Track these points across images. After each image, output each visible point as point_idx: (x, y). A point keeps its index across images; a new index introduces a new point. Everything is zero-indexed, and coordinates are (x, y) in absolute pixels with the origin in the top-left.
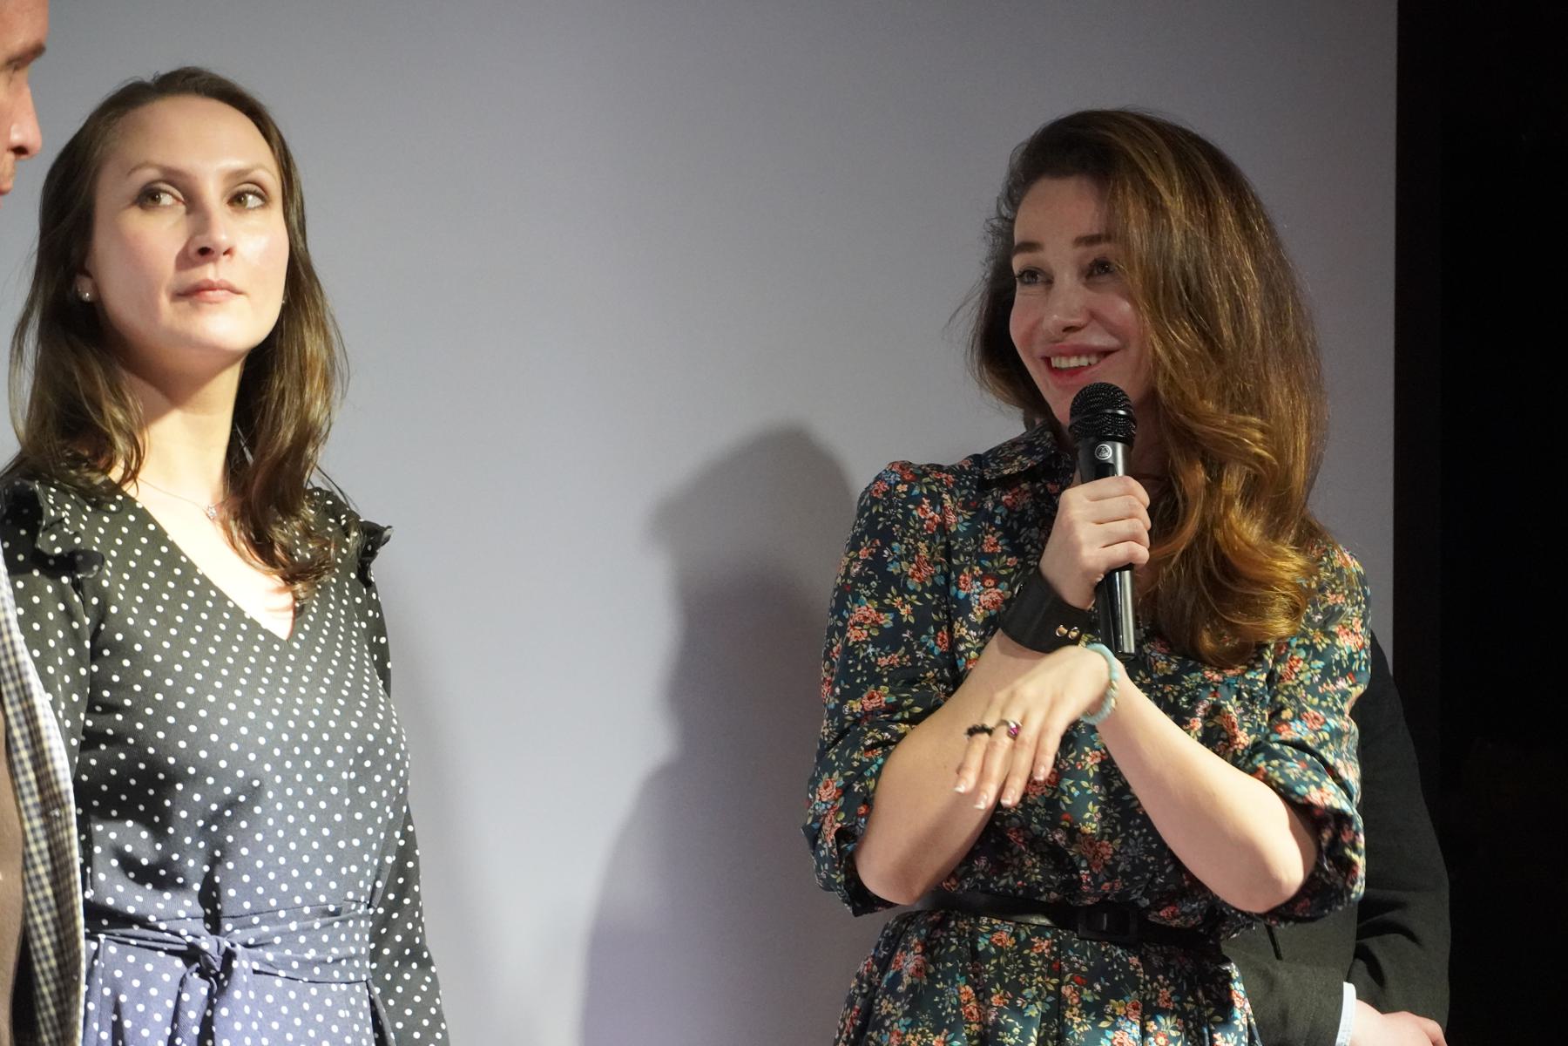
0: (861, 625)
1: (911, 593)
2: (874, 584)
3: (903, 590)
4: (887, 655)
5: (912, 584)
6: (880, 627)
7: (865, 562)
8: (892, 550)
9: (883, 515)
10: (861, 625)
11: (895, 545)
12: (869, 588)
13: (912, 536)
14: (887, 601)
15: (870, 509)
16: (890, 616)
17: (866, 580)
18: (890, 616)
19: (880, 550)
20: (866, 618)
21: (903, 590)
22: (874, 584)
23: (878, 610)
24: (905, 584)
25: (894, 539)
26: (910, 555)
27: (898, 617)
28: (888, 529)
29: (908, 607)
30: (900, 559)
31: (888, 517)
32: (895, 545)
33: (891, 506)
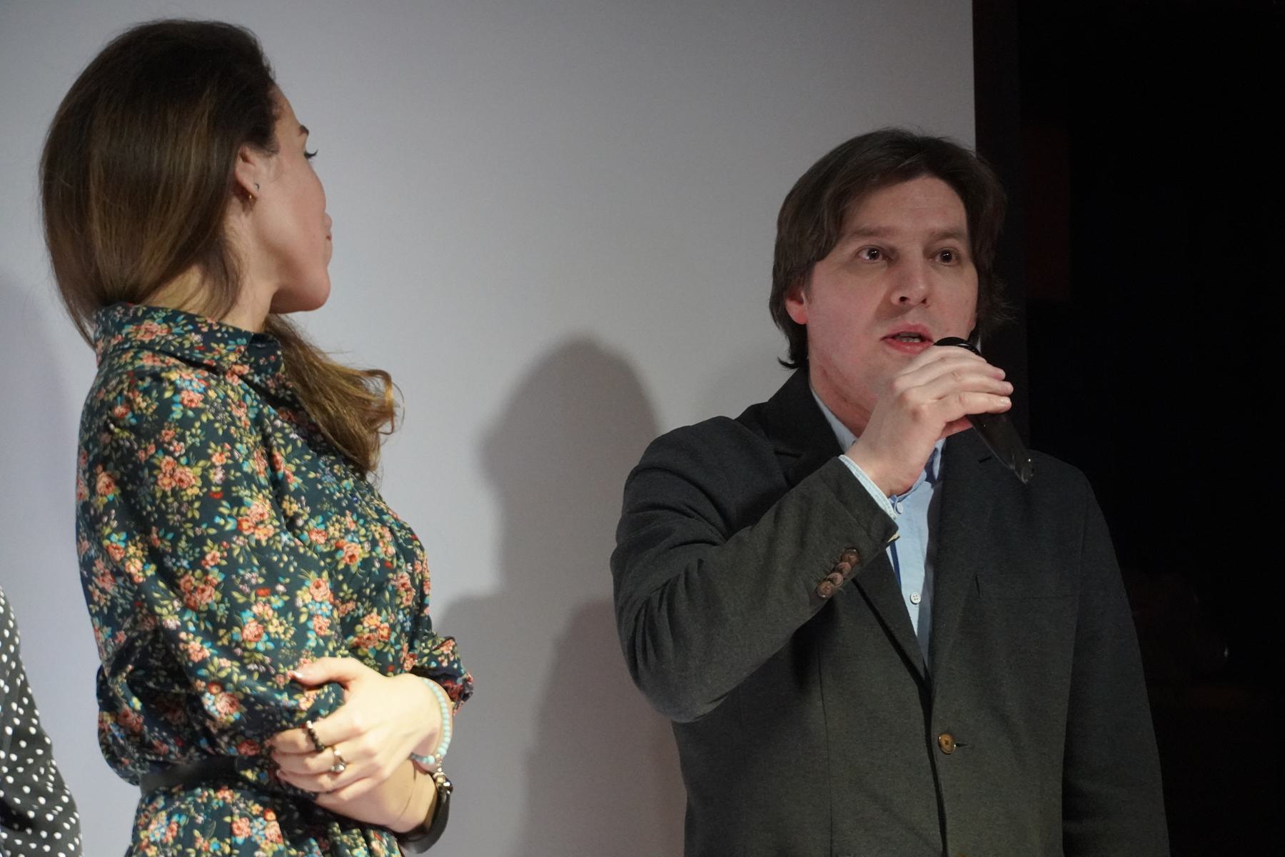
0: (262, 522)
1: (265, 488)
7: (226, 468)
20: (262, 515)
28: (226, 432)
30: (247, 458)
31: (222, 422)
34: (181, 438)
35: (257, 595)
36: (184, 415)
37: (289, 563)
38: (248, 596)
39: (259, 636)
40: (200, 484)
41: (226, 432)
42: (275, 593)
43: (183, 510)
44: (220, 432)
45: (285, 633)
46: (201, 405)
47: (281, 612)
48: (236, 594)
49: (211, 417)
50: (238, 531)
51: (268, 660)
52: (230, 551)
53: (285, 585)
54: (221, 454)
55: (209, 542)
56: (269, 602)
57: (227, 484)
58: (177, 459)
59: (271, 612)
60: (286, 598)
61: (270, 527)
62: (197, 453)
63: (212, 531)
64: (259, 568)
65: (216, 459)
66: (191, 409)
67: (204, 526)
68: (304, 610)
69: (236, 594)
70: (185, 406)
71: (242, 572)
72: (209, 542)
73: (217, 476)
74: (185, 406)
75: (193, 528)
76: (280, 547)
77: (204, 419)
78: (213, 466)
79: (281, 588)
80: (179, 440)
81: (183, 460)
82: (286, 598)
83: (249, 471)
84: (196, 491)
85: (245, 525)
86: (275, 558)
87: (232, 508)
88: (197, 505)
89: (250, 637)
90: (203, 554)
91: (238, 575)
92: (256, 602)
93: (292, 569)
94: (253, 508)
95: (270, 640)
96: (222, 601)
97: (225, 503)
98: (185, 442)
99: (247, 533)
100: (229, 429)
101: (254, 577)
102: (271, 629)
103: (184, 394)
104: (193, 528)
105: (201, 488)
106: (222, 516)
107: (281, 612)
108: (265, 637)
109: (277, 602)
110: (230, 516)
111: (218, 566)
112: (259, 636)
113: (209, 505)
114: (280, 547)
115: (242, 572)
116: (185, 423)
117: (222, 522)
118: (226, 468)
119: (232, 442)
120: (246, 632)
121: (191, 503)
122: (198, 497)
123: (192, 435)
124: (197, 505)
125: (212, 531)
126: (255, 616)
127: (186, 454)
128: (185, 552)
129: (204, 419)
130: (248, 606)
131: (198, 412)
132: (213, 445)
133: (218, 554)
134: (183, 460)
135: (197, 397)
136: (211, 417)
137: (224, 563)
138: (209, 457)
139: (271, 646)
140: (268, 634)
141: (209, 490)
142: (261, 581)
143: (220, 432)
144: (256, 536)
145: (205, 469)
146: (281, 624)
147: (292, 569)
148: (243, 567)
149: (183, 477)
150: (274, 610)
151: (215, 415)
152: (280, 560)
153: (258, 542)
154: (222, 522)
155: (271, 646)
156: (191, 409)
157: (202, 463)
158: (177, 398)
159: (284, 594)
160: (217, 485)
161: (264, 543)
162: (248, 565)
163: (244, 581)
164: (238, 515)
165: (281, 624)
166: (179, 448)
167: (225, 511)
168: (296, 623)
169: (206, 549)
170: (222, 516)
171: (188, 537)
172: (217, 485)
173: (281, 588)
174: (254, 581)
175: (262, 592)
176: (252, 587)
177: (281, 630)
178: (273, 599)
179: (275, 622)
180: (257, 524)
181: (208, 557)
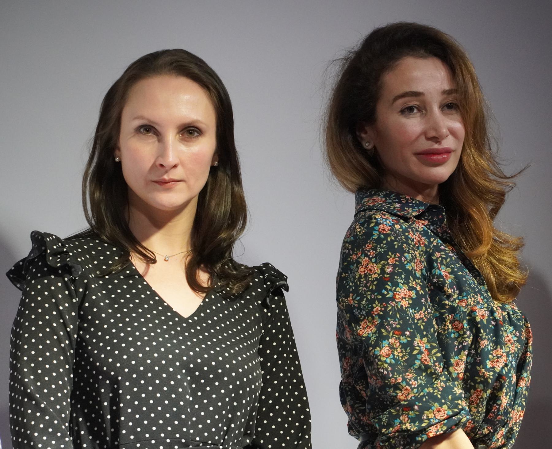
0: (405, 298)
1: (418, 279)
2: (403, 276)
3: (415, 278)
4: (418, 312)
5: (418, 274)
6: (412, 298)
7: (394, 266)
8: (405, 258)
9: (395, 241)
11: (406, 255)
12: (402, 279)
13: (413, 249)
14: (410, 284)
16: (414, 292)
17: (399, 274)
18: (414, 292)
19: (400, 258)
21: (415, 278)
22: (403, 276)
24: (415, 273)
25: (405, 252)
26: (414, 258)
27: (417, 292)
28: (400, 247)
29: (418, 286)
30: (410, 261)
32: (406, 255)
33: (398, 236)
34: (375, 249)
35: (394, 334)
36: (379, 236)
38: (389, 332)
39: (389, 355)
40: (379, 272)
41: (400, 247)
42: (404, 335)
43: (368, 285)
44: (396, 247)
45: (402, 357)
46: (389, 232)
47: (404, 346)
48: (383, 330)
49: (393, 239)
50: (393, 299)
51: (390, 369)
52: (386, 308)
54: (393, 259)
55: (376, 302)
56: (399, 339)
57: (393, 274)
58: (370, 259)
59: (398, 344)
60: (409, 339)
62: (381, 257)
63: (380, 297)
64: (399, 320)
65: (391, 261)
66: (383, 234)
67: (376, 294)
68: (417, 348)
69: (383, 330)
70: (380, 232)
71: (389, 319)
72: (376, 302)
73: (389, 269)
74: (380, 232)
75: (371, 295)
77: (389, 239)
78: (388, 264)
79: (407, 333)
80: (373, 250)
81: (373, 260)
82: (409, 339)
83: (410, 268)
84: (376, 276)
85: (397, 297)
87: (392, 287)
88: (375, 283)
89: (384, 354)
90: (373, 308)
91: (387, 320)
92: (392, 337)
94: (403, 289)
95: (394, 358)
96: (375, 333)
97: (389, 283)
98: (376, 250)
99: (397, 301)
100: (402, 245)
101: (395, 324)
102: (396, 353)
103: (381, 227)
104: (371, 295)
105: (379, 275)
106: (386, 289)
107: (404, 346)
108: (391, 356)
109: (404, 340)
110: (391, 290)
111: (378, 314)
112: (389, 355)
113: (381, 283)
115: (389, 319)
116: (379, 241)
117: (386, 293)
118: (394, 266)
119: (402, 252)
120: (383, 351)
121: (372, 282)
122: (376, 278)
123: (381, 248)
124: (375, 283)
125: (380, 297)
126: (389, 344)
127: (375, 257)
128: (364, 307)
129: (389, 239)
130: (387, 338)
131: (387, 235)
132: (390, 254)
133: (379, 309)
134: (373, 260)
135: (387, 228)
136: (393, 239)
137: (382, 313)
139: (393, 362)
140: (394, 355)
141: (383, 275)
142: (398, 326)
143: (396, 247)
144: (401, 303)
145: (384, 265)
146: (402, 352)
148: (391, 317)
149: (372, 268)
150: (400, 343)
151: (395, 237)
154: (386, 293)
155: (393, 362)
156: (383, 234)
157: (382, 262)
158: (377, 228)
159: (408, 337)
160: (388, 274)
162: (394, 317)
163: (389, 324)
164: (395, 290)
165: (402, 352)
166: (372, 253)
168: (410, 354)
169: (374, 305)
170: (386, 289)
171: (367, 299)
172: (388, 274)
173: (407, 333)
174: (394, 326)
175: (397, 332)
176: (392, 329)
177: (400, 355)
178: (402, 338)
179: (399, 350)
181: (375, 310)
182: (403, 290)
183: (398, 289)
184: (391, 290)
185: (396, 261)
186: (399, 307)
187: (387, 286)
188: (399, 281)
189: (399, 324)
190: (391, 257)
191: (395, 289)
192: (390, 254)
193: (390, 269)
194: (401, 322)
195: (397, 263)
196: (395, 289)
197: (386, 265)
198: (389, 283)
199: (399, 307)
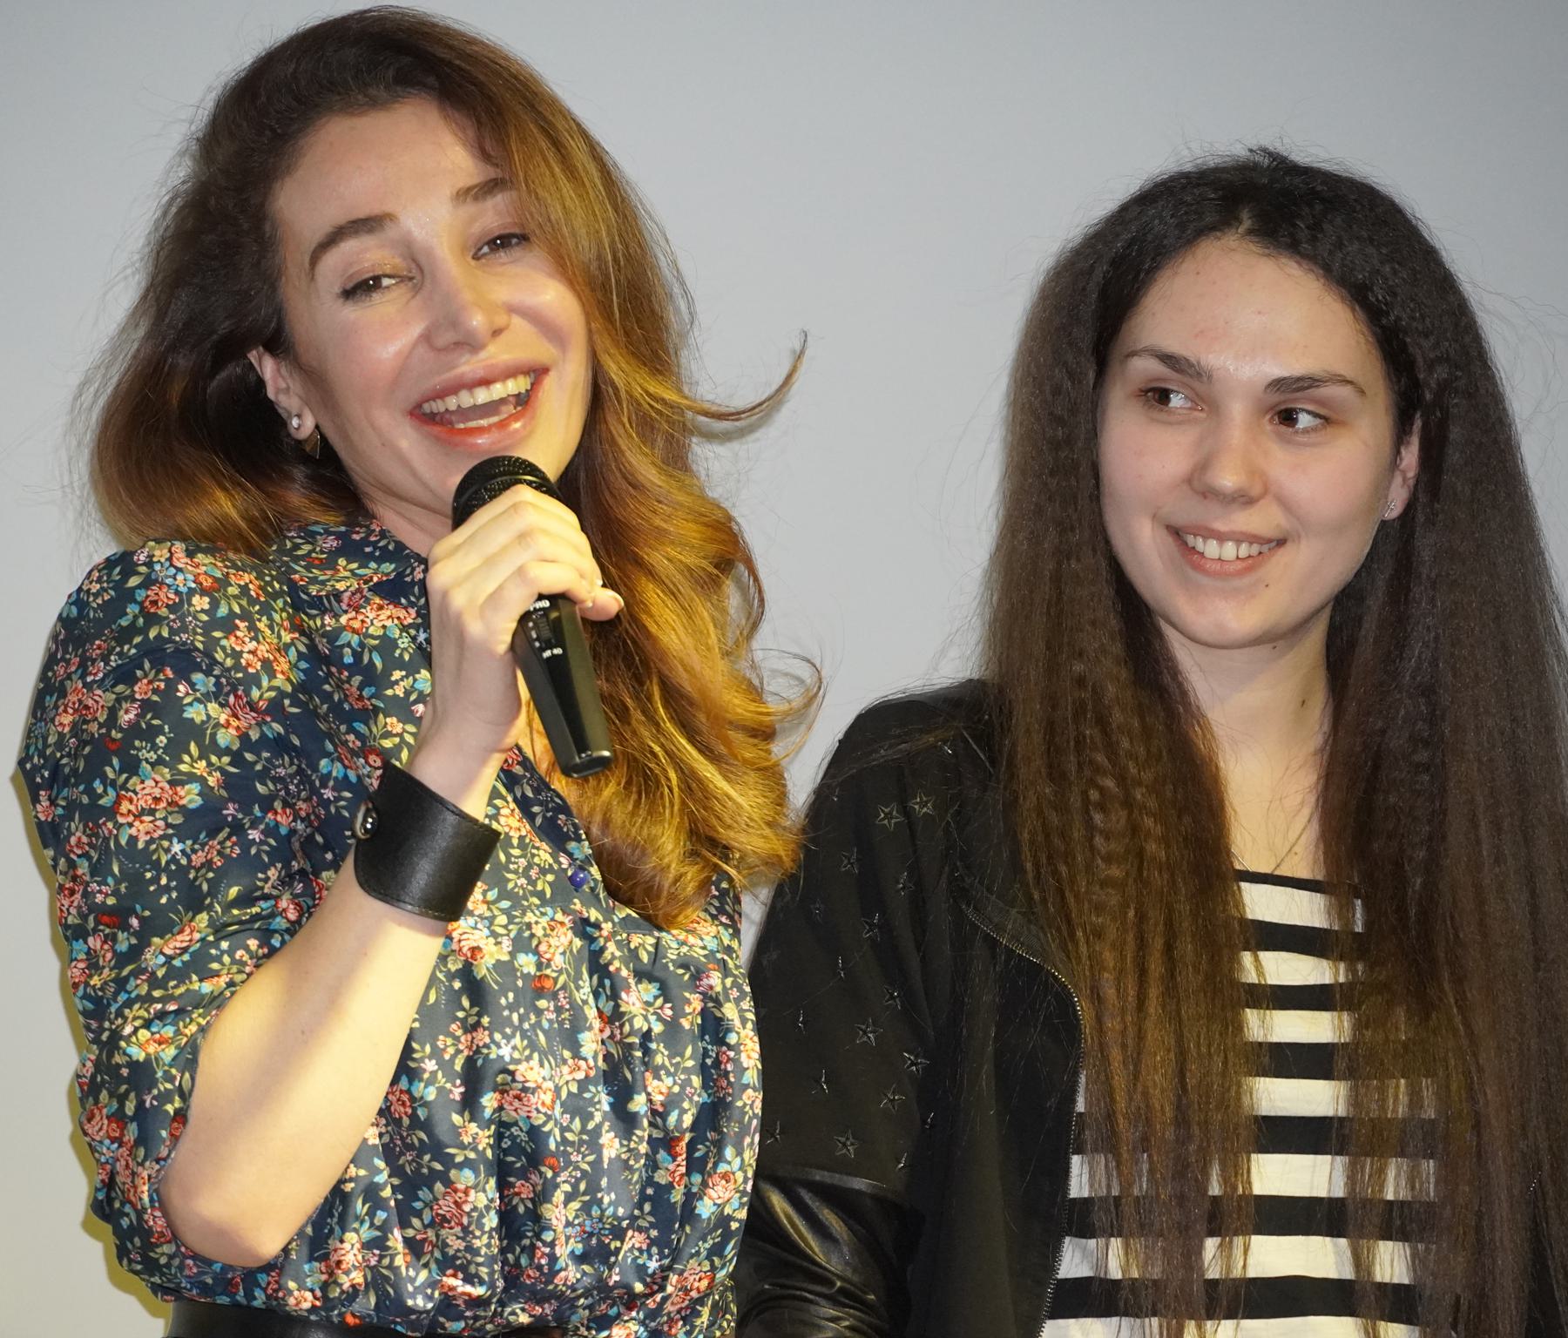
0: (152, 812)
7: (146, 705)
8: (192, 685)
10: (152, 812)
15: (144, 631)
19: (171, 686)
20: (157, 800)
23: (172, 783)
30: (205, 699)
37: (167, 889)
53: (142, 920)
57: (134, 731)
61: (161, 823)
64: (118, 882)
65: (141, 690)
73: (127, 716)
76: (164, 859)
85: (125, 807)
86: (148, 875)
93: (164, 900)
94: (149, 783)
97: (115, 761)
110: (113, 783)
114: (164, 859)
138: (131, 680)
144: (133, 831)
147: (164, 900)
152: (156, 880)
153: (133, 840)
160: (121, 730)
161: (141, 845)
164: (124, 787)
167: (111, 775)
172: (121, 730)
180: (143, 812)
182: (150, 786)
183: (134, 779)
184: (113, 783)
185: (155, 691)
186: (123, 842)
187: (108, 769)
188: (144, 754)
189: (116, 893)
190: (146, 676)
191: (127, 780)
192: (147, 665)
193: (131, 716)
194: (123, 888)
195: (155, 698)
196: (127, 780)
197: (126, 699)
198: (115, 761)
199: (123, 842)
